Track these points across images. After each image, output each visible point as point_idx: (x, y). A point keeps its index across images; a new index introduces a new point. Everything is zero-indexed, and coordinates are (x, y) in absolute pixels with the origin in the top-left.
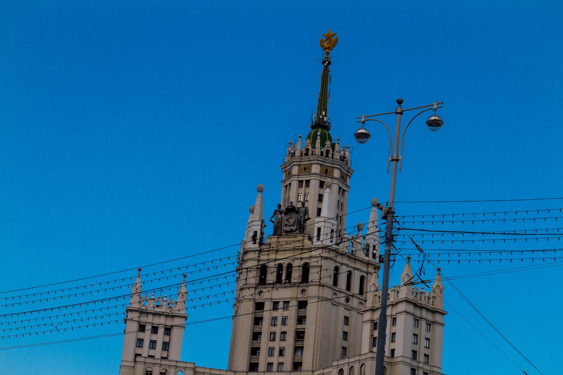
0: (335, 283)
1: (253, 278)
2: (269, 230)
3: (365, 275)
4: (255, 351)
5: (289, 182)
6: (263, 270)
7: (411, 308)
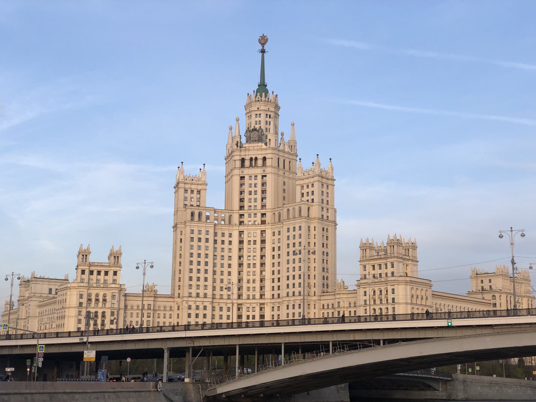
0: (278, 166)
1: (238, 164)
2: (244, 140)
3: (291, 160)
4: (242, 200)
5: (250, 115)
6: (243, 160)
7: (320, 179)
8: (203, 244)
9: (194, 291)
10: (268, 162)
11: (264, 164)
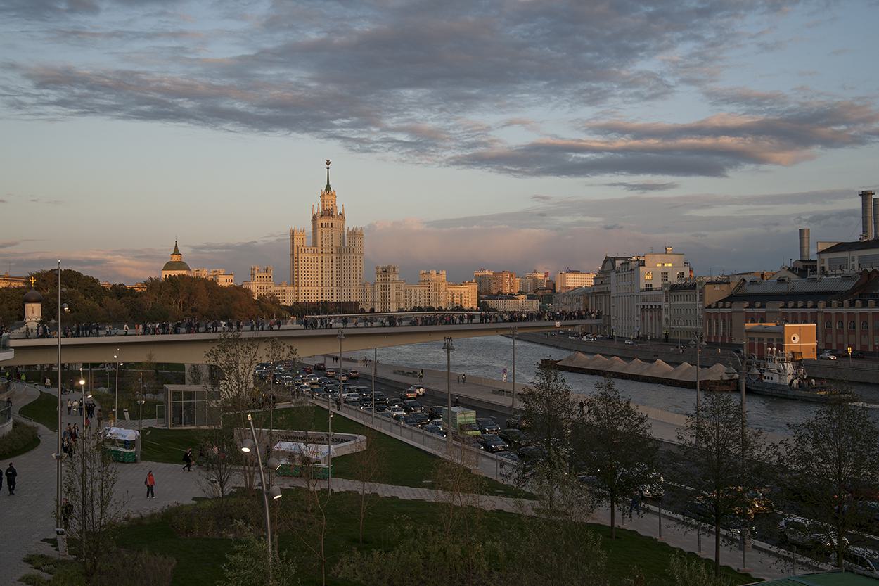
1: (320, 226)
6: (322, 224)
8: (306, 263)
9: (303, 284)
10: (334, 226)
11: (332, 226)
